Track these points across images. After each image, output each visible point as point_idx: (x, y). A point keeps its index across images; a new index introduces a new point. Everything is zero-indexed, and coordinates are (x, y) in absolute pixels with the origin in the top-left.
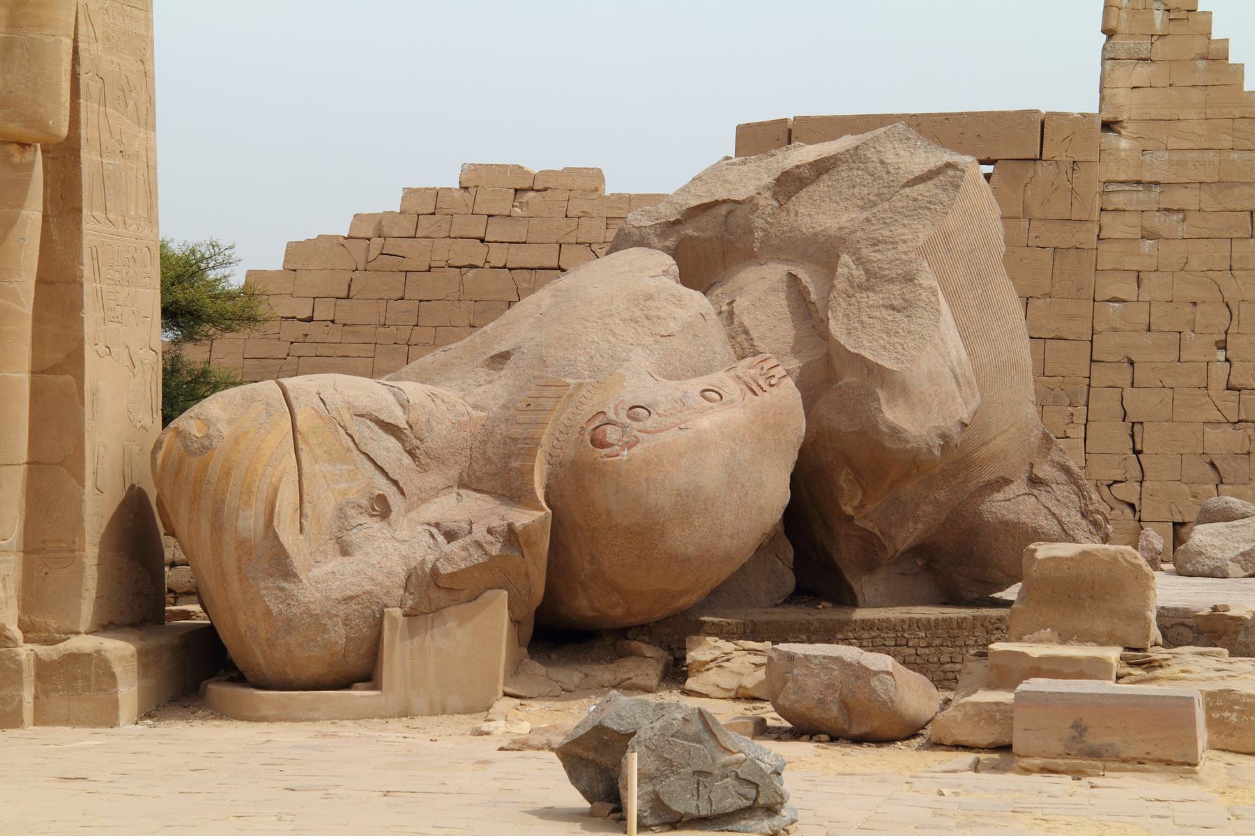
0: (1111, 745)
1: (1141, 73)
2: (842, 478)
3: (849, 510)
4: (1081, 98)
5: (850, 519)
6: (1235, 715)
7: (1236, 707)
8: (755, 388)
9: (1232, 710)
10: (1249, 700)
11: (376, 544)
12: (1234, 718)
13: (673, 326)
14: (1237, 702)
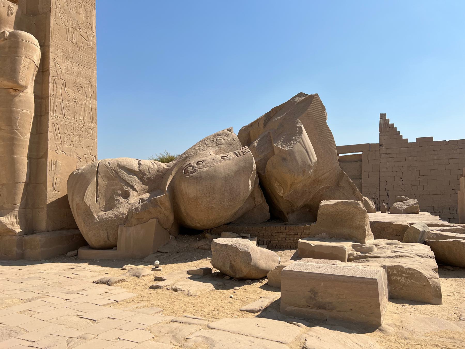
0: (331, 303)
1: (386, 137)
2: (276, 184)
3: (280, 194)
5: (282, 197)
6: (403, 278)
7: (404, 275)
8: (238, 155)
9: (401, 276)
10: (410, 272)
12: (403, 280)
13: (223, 141)
14: (404, 272)
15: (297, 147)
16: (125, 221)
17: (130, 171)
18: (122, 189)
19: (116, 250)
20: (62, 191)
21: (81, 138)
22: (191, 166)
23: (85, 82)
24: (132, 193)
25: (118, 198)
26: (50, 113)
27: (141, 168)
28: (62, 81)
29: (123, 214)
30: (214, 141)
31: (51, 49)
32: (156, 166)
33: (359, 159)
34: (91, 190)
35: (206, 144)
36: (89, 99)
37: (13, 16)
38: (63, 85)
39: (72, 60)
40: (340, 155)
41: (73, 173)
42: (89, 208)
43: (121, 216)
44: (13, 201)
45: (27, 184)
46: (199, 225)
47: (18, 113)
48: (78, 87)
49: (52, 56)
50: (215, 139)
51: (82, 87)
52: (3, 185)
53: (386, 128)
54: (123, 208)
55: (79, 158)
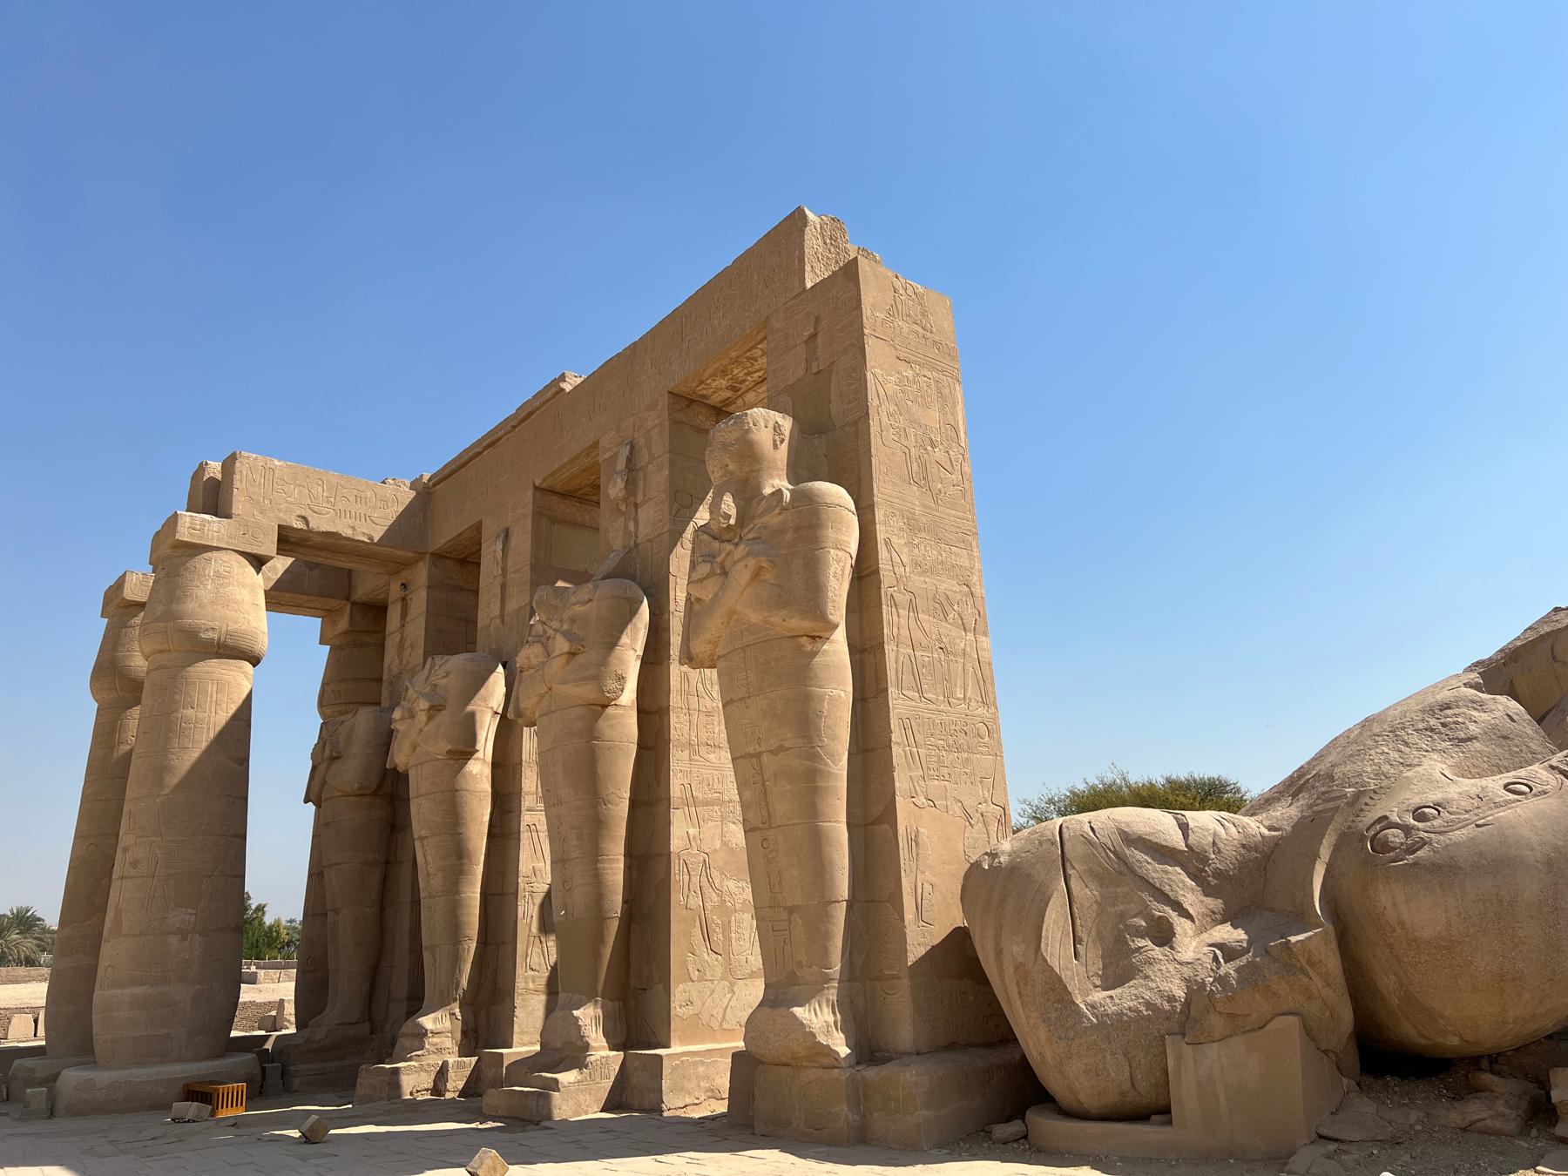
11: (1158, 967)
17: (1163, 853)
18: (1145, 912)
19: (1170, 1123)
21: (965, 755)
22: (1397, 826)
23: (957, 588)
24: (1181, 926)
25: (1141, 943)
26: (892, 690)
27: (1191, 840)
28: (908, 597)
29: (1171, 999)
30: (1432, 730)
31: (879, 515)
32: (1233, 830)
34: (1055, 919)
35: (1406, 744)
36: (970, 636)
38: (913, 607)
39: (924, 535)
41: (976, 866)
42: (1060, 979)
43: (1167, 1006)
44: (823, 959)
45: (851, 904)
46: (1454, 1041)
47: (821, 699)
48: (942, 606)
49: (881, 533)
50: (1433, 722)
51: (951, 605)
52: (792, 910)
55: (968, 817)
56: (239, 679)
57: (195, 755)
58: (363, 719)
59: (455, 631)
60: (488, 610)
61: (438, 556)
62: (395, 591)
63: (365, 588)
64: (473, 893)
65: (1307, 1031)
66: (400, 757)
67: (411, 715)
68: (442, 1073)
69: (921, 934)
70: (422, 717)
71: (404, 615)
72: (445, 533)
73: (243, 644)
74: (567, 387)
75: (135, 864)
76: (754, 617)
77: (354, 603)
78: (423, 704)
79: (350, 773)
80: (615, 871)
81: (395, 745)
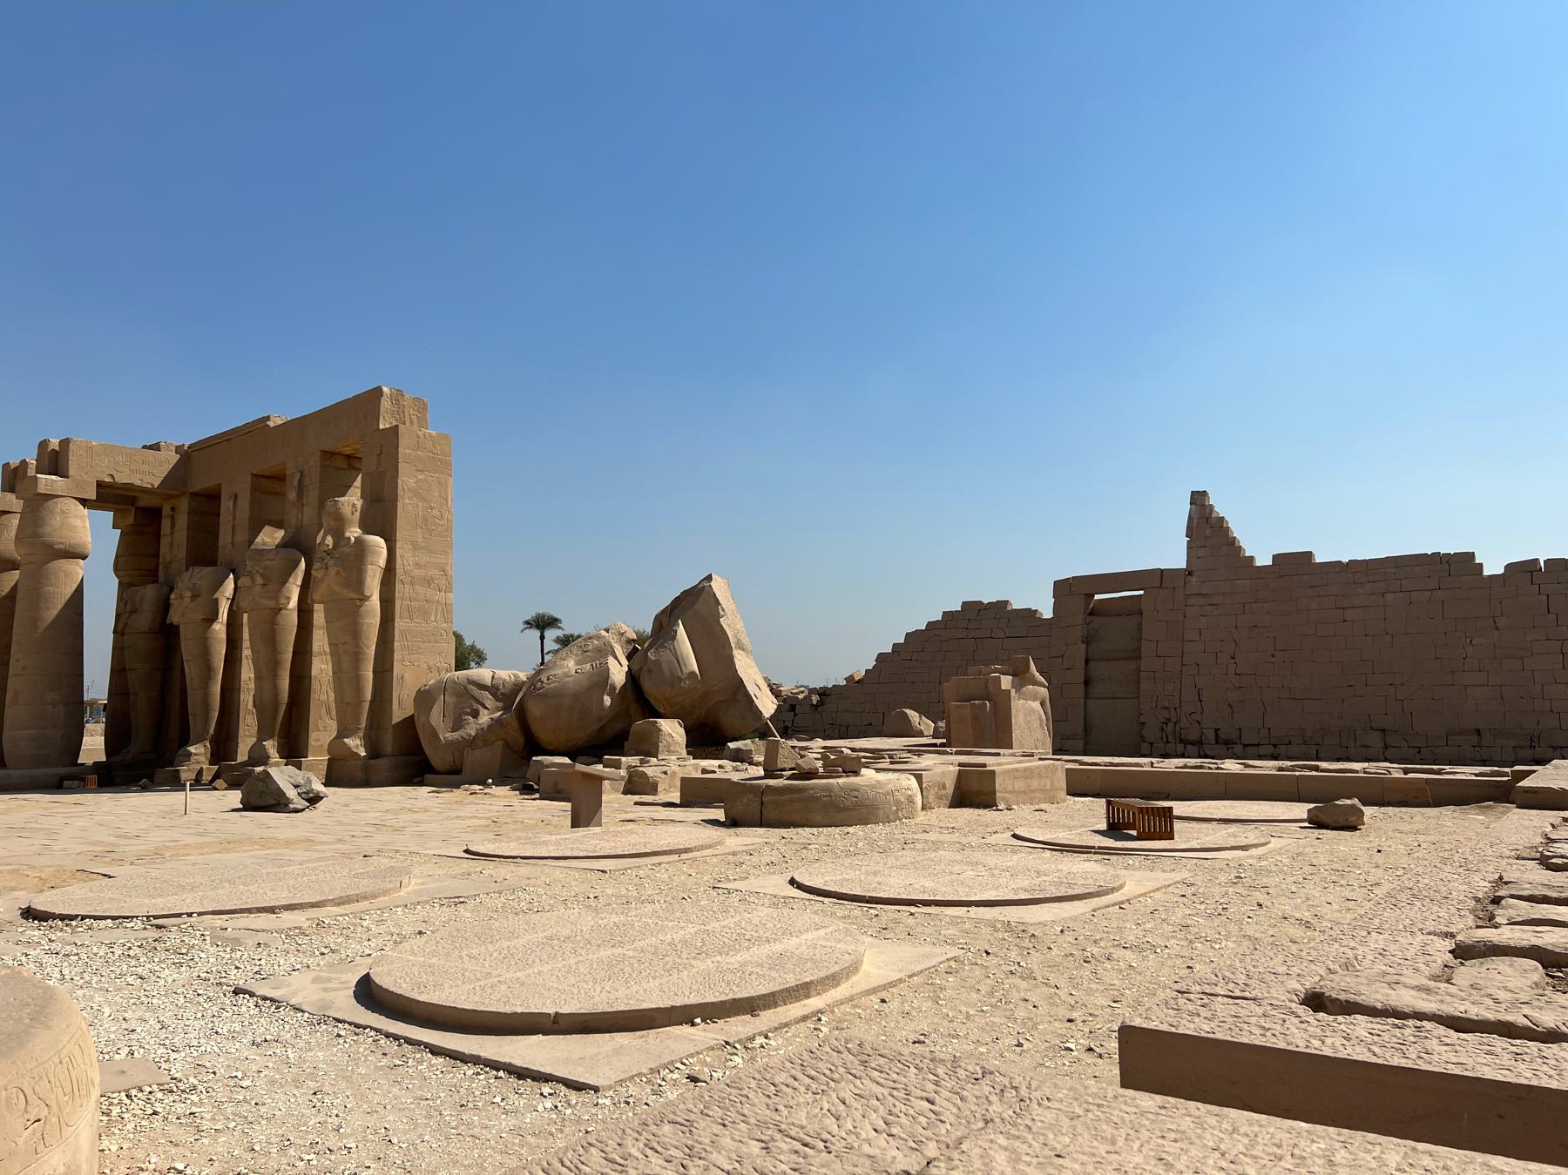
1: (1201, 552)
4: (1181, 564)
15: (665, 655)
16: (472, 743)
20: (409, 711)
24: (483, 711)
31: (398, 544)
33: (1131, 609)
37: (358, 514)
38: (412, 583)
40: (1097, 597)
44: (358, 721)
48: (428, 582)
49: (399, 552)
53: (1206, 526)
54: (471, 729)
55: (430, 668)
56: (78, 569)
57: (55, 612)
58: (150, 593)
59: (205, 553)
60: (224, 538)
61: (194, 495)
62: (166, 510)
63: (144, 502)
64: (217, 688)
65: (507, 745)
66: (175, 617)
67: (182, 598)
68: (200, 772)
69: (398, 715)
70: (187, 600)
71: (173, 526)
72: (200, 483)
73: (78, 551)
74: (271, 424)
75: (24, 668)
76: (337, 589)
77: (138, 509)
78: (188, 594)
79: (144, 620)
80: (285, 683)
81: (172, 611)
